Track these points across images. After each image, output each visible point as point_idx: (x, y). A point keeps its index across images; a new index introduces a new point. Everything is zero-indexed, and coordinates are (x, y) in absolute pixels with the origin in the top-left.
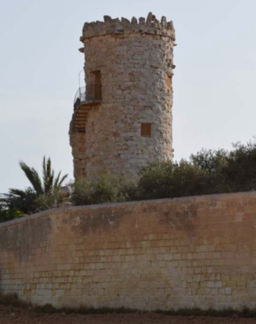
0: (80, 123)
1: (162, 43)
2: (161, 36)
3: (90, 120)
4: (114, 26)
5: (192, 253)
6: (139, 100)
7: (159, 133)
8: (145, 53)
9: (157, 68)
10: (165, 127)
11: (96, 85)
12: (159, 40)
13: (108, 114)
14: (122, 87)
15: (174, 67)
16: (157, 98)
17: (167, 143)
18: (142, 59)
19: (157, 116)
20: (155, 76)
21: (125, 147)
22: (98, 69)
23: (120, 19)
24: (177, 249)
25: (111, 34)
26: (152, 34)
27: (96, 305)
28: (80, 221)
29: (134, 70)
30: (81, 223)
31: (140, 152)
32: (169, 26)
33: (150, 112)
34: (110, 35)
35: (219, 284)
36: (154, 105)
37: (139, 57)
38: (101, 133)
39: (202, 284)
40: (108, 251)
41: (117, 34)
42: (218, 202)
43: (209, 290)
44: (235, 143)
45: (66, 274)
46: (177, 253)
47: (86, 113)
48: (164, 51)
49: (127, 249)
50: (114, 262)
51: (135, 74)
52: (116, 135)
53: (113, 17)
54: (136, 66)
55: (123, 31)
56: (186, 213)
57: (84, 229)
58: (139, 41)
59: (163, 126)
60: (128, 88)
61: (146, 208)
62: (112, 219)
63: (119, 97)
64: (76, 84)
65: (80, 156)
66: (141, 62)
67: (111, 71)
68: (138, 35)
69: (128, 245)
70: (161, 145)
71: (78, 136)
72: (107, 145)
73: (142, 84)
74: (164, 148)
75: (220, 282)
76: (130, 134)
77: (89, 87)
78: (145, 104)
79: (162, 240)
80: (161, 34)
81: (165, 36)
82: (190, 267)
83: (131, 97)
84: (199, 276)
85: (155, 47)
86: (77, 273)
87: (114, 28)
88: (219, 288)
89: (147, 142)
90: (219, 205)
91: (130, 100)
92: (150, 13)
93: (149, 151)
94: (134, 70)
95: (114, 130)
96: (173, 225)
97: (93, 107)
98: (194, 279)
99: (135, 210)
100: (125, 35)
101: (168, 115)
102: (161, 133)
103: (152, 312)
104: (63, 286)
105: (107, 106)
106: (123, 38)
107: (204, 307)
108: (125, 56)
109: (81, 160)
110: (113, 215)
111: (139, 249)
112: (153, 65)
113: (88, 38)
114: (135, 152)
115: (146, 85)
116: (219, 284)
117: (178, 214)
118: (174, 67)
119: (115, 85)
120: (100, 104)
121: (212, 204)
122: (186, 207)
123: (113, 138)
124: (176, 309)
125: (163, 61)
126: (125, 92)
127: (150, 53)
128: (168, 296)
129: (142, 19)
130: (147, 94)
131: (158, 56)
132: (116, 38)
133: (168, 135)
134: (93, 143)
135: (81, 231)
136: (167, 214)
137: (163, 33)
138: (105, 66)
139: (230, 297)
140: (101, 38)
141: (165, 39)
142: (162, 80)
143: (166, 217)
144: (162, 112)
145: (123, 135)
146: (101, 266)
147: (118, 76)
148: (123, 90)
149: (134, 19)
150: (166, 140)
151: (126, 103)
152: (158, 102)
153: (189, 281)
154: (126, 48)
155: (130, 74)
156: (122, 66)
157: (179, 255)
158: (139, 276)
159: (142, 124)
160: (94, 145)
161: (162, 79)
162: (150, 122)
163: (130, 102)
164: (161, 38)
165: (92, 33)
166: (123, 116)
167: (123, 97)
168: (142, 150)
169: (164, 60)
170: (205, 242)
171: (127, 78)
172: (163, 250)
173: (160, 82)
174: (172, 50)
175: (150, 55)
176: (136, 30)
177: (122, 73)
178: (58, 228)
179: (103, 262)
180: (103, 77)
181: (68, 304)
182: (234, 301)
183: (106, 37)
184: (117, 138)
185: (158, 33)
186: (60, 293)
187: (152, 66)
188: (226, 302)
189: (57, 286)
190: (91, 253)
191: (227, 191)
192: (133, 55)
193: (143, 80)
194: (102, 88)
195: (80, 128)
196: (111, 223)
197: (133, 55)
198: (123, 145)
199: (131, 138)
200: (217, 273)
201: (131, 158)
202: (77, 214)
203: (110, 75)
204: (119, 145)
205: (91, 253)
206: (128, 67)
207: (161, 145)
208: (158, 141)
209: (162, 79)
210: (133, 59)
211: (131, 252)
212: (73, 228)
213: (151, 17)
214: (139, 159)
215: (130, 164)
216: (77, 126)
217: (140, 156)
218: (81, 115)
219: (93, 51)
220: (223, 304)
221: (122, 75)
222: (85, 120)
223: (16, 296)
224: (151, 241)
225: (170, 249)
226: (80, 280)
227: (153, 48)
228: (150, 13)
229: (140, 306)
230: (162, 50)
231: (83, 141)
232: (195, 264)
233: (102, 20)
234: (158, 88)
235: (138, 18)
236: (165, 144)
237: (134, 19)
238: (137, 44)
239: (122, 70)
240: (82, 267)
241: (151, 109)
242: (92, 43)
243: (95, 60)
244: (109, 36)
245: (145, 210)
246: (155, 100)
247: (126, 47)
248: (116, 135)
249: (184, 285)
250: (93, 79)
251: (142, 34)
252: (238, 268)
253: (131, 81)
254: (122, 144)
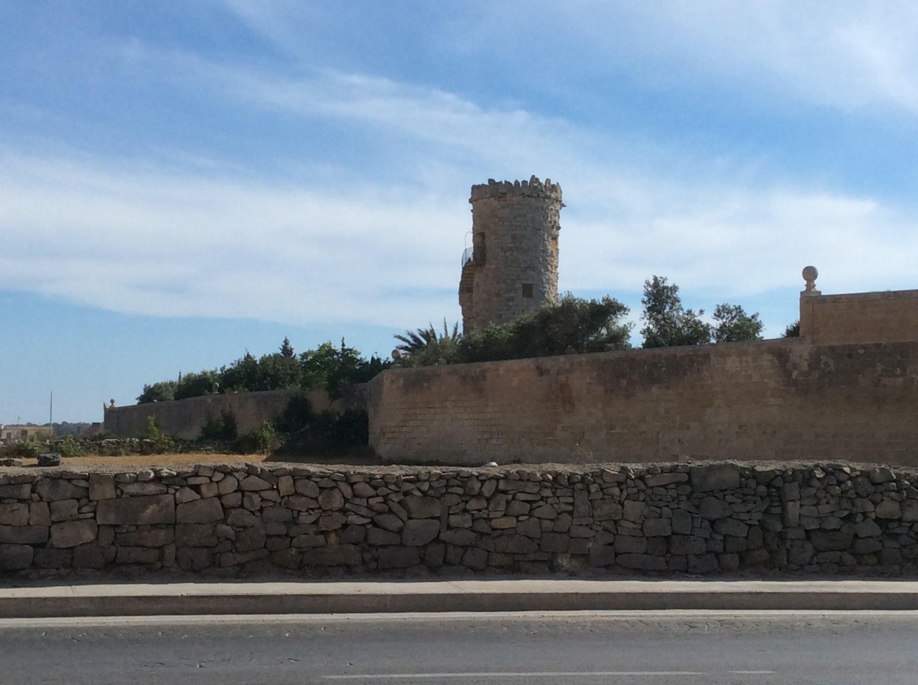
3: (476, 280)
29: (516, 232)
53: (497, 181)
76: (511, 295)
77: (476, 247)
92: (533, 176)
101: (552, 276)
129: (524, 182)
149: (517, 182)
174: (558, 211)
196: (425, 384)
199: (512, 299)
203: (494, 237)
211: (439, 411)
213: (534, 179)
228: (533, 176)
233: (487, 183)
237: (517, 182)
250: (479, 239)
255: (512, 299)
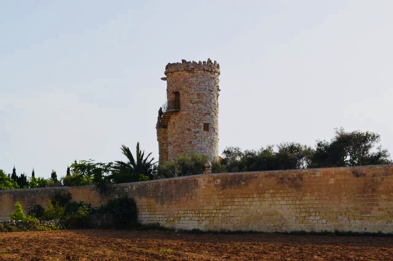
0: (164, 122)
1: (215, 77)
2: (214, 72)
3: (172, 120)
4: (188, 66)
5: (300, 200)
6: (203, 110)
7: (213, 130)
8: (206, 82)
9: (212, 91)
10: (216, 125)
11: (175, 100)
12: (213, 75)
13: (184, 118)
14: (193, 102)
15: (220, 90)
16: (212, 109)
17: (217, 135)
18: (204, 86)
19: (212, 119)
20: (212, 96)
21: (194, 137)
22: (177, 91)
23: (192, 62)
24: (289, 198)
25: (186, 70)
26: (210, 71)
27: (232, 229)
28: (221, 182)
29: (200, 92)
30: (221, 183)
31: (203, 140)
32: (218, 67)
33: (208, 117)
34: (186, 71)
35: (318, 218)
36: (211, 113)
37: (203, 84)
38: (180, 128)
39: (306, 218)
40: (241, 199)
41: (190, 71)
42: (317, 173)
43: (311, 221)
44: (316, 139)
45: (211, 212)
46: (290, 200)
47: (169, 117)
48: (216, 81)
49: (253, 198)
50: (245, 205)
51: (200, 94)
52: (189, 130)
53: (187, 61)
54: (201, 89)
55: (194, 69)
56: (295, 179)
57: (224, 186)
58: (202, 75)
59: (215, 125)
60: (197, 102)
61: (268, 175)
62: (243, 181)
63: (191, 108)
64: (160, 99)
65: (163, 142)
66: (204, 87)
67: (186, 92)
68: (202, 72)
69: (255, 196)
70: (214, 136)
71: (162, 130)
72: (184, 136)
73: (204, 100)
74: (215, 138)
75: (319, 217)
76: (197, 130)
78: (206, 112)
79: (278, 193)
80: (214, 71)
81: (216, 72)
82: (298, 208)
83: (198, 108)
84: (305, 213)
85: (212, 79)
86: (218, 211)
87: (188, 67)
88: (318, 220)
89: (207, 134)
90: (318, 174)
91: (197, 110)
92: (209, 59)
93: (208, 140)
94: (200, 92)
95: (188, 127)
96: (286, 185)
97: (174, 113)
98: (301, 215)
99: (260, 176)
100: (195, 72)
102: (214, 129)
103: (272, 233)
104: (207, 219)
105: (183, 113)
106: (193, 73)
107: (308, 230)
108: (194, 84)
109: (163, 144)
110: (244, 179)
111: (262, 198)
112: (210, 89)
113: (171, 72)
114: (200, 140)
115: (207, 101)
116: (318, 218)
117: (289, 179)
118: (220, 90)
119: (189, 101)
120: (179, 111)
121: (313, 173)
122: (295, 175)
123: (187, 132)
124: (289, 232)
125: (215, 87)
126: (195, 105)
127: (209, 82)
128: (283, 224)
129: (204, 62)
130: (207, 106)
131: (213, 84)
132: (189, 73)
133: (217, 130)
134: (174, 134)
135: (221, 187)
136: (282, 179)
137: (215, 70)
138: (183, 89)
139: (325, 225)
140: (180, 72)
141: (216, 74)
142: (215, 98)
143: (282, 180)
144: (215, 117)
145: (193, 130)
146: (235, 207)
147: (190, 95)
148: (193, 104)
149: (200, 62)
150: (216, 133)
151: (195, 111)
152: (213, 111)
153: (297, 216)
154: (195, 79)
155: (197, 94)
156: (193, 89)
157: (291, 201)
158: (263, 213)
159: (204, 123)
160: (174, 136)
161: (215, 97)
162: (209, 123)
163: (197, 111)
164: (214, 74)
165: (171, 69)
166: (193, 119)
167: (193, 108)
168: (204, 139)
169: (216, 86)
170: (308, 194)
171: (196, 97)
172: (279, 199)
173: (214, 99)
175: (209, 83)
176: (202, 69)
177: (193, 93)
178: (204, 185)
179: (237, 205)
180: (181, 95)
181: (212, 228)
182: (328, 227)
183: (183, 72)
184: (190, 132)
185: (213, 71)
186: (204, 223)
187: (209, 90)
188: (323, 227)
189: (203, 218)
190: (229, 200)
191: (325, 167)
192: (199, 83)
193: (204, 97)
194: (180, 102)
195: (164, 125)
196: (243, 183)
197: (199, 83)
198: (194, 136)
199: (198, 132)
200: (317, 212)
201: (198, 143)
202: (218, 178)
203: (186, 95)
204: (191, 136)
205: (229, 200)
206: (197, 90)
207: (214, 136)
208: (212, 134)
209: (215, 97)
210: (199, 85)
211: (257, 199)
212: (216, 186)
213: (209, 61)
214: (202, 144)
215: (198, 147)
216: (162, 124)
217: (203, 142)
218: (166, 118)
219: (174, 80)
220: (320, 228)
221: (193, 94)
222: (168, 121)
223: (158, 224)
224: (271, 193)
225: (284, 198)
226: (220, 215)
227: (210, 79)
228: (209, 59)
229: (263, 229)
230: (215, 81)
231: (165, 133)
232: (301, 207)
233: (181, 62)
234: (213, 103)
235: (202, 62)
236: (216, 136)
237: (200, 62)
238: (202, 77)
239: (193, 92)
240: (222, 208)
241: (209, 115)
242: (173, 75)
243: (176, 85)
244: (185, 72)
245: (266, 176)
246: (211, 109)
247: (195, 78)
248: (189, 130)
249: (294, 218)
250: (173, 96)
251: (205, 71)
252: (331, 209)
253: (198, 98)
254: (193, 135)
255: (198, 132)
